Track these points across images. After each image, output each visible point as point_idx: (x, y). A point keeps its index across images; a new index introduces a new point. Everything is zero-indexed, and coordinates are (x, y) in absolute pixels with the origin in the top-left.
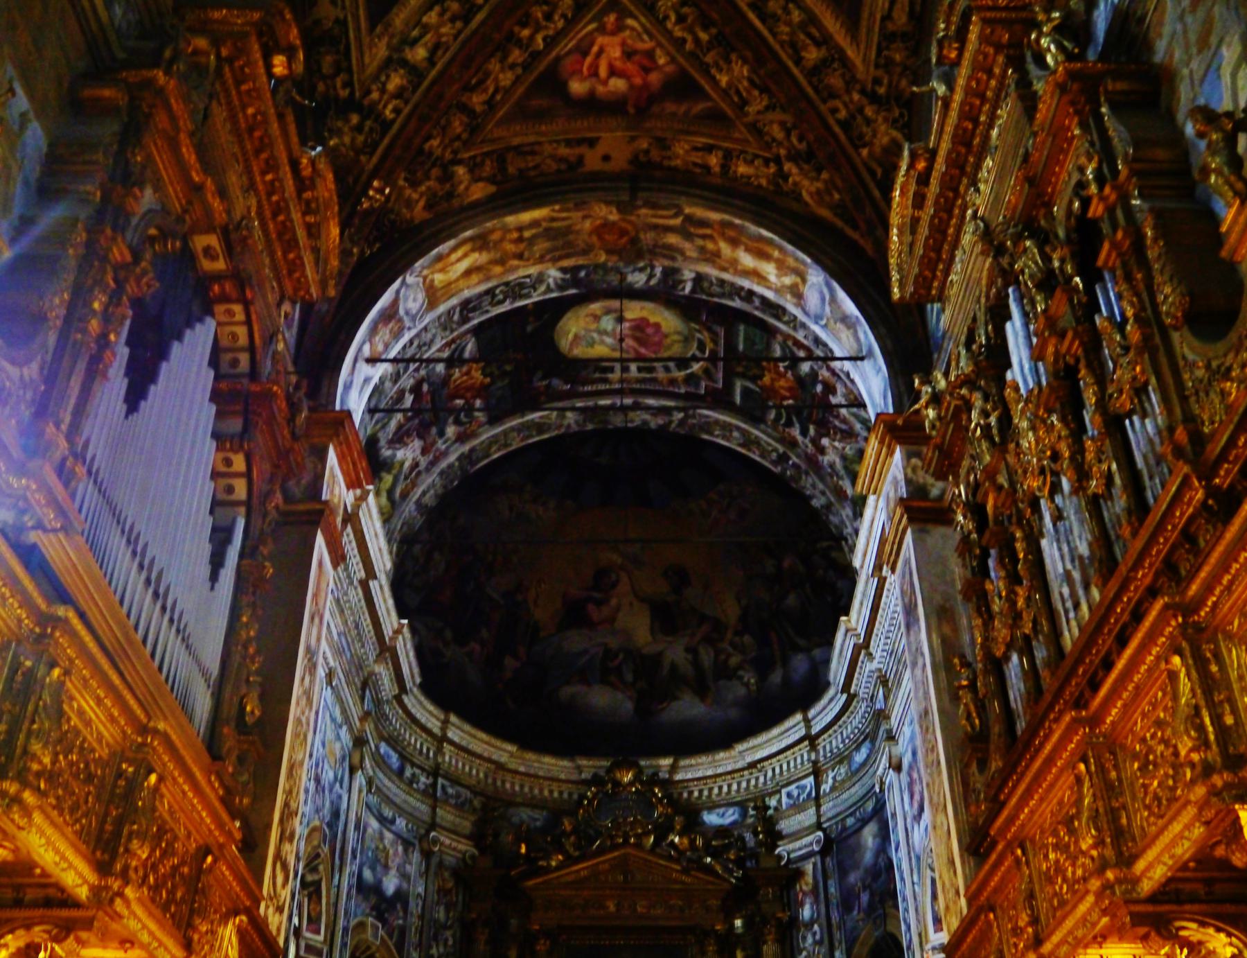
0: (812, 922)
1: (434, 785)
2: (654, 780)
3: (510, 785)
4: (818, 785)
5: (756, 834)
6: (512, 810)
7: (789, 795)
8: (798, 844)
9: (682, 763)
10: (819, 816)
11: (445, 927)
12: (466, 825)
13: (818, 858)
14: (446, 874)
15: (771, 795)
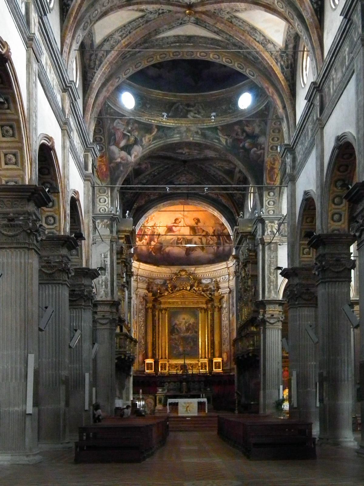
0: (226, 308)
1: (137, 278)
2: (190, 274)
3: (154, 275)
4: (229, 277)
5: (214, 287)
6: (155, 280)
7: (222, 278)
8: (223, 290)
9: (197, 269)
10: (229, 285)
11: (142, 310)
12: (145, 286)
13: (228, 294)
14: (141, 298)
15: (218, 277)
